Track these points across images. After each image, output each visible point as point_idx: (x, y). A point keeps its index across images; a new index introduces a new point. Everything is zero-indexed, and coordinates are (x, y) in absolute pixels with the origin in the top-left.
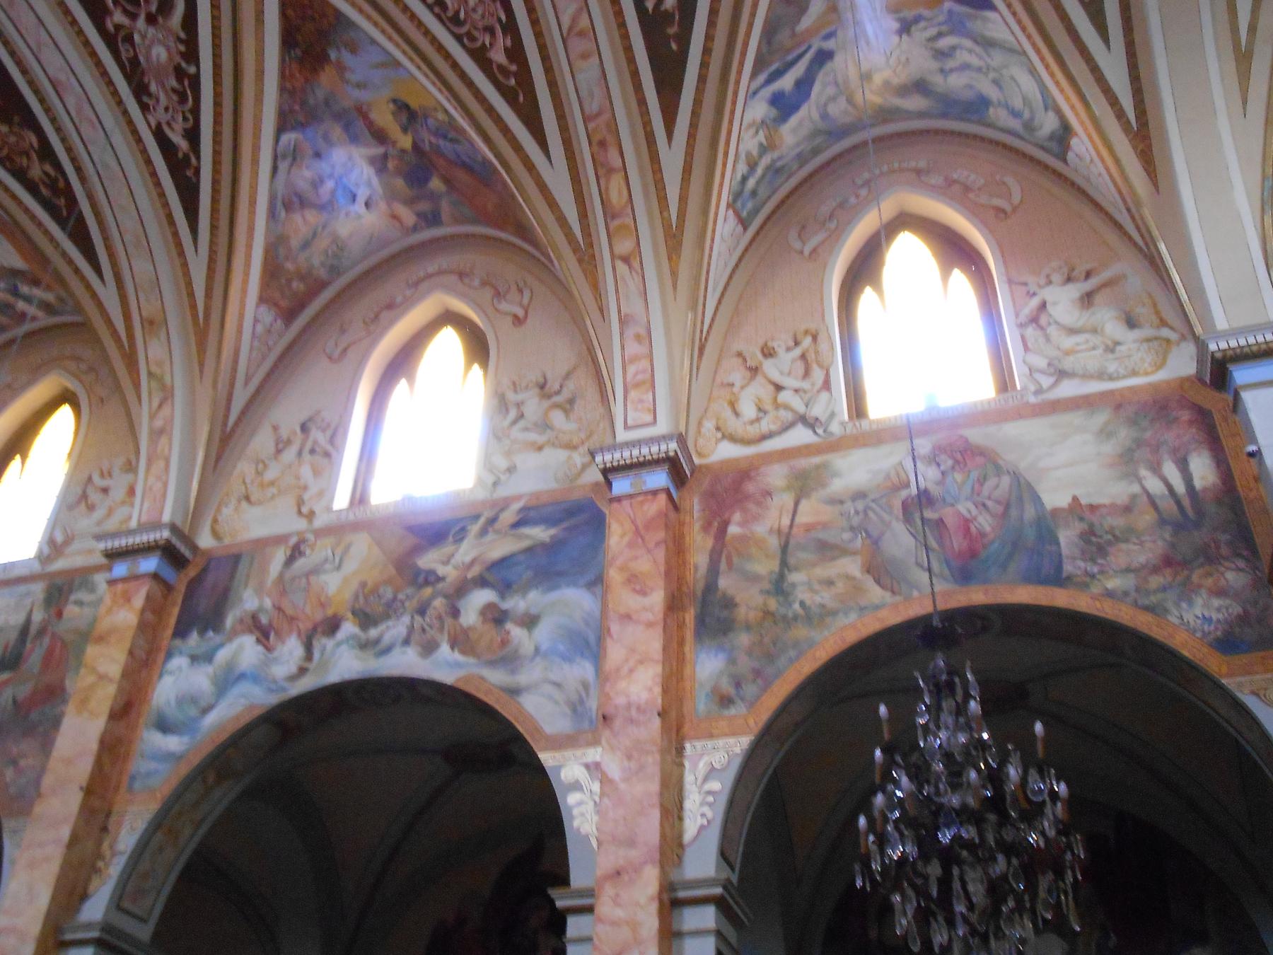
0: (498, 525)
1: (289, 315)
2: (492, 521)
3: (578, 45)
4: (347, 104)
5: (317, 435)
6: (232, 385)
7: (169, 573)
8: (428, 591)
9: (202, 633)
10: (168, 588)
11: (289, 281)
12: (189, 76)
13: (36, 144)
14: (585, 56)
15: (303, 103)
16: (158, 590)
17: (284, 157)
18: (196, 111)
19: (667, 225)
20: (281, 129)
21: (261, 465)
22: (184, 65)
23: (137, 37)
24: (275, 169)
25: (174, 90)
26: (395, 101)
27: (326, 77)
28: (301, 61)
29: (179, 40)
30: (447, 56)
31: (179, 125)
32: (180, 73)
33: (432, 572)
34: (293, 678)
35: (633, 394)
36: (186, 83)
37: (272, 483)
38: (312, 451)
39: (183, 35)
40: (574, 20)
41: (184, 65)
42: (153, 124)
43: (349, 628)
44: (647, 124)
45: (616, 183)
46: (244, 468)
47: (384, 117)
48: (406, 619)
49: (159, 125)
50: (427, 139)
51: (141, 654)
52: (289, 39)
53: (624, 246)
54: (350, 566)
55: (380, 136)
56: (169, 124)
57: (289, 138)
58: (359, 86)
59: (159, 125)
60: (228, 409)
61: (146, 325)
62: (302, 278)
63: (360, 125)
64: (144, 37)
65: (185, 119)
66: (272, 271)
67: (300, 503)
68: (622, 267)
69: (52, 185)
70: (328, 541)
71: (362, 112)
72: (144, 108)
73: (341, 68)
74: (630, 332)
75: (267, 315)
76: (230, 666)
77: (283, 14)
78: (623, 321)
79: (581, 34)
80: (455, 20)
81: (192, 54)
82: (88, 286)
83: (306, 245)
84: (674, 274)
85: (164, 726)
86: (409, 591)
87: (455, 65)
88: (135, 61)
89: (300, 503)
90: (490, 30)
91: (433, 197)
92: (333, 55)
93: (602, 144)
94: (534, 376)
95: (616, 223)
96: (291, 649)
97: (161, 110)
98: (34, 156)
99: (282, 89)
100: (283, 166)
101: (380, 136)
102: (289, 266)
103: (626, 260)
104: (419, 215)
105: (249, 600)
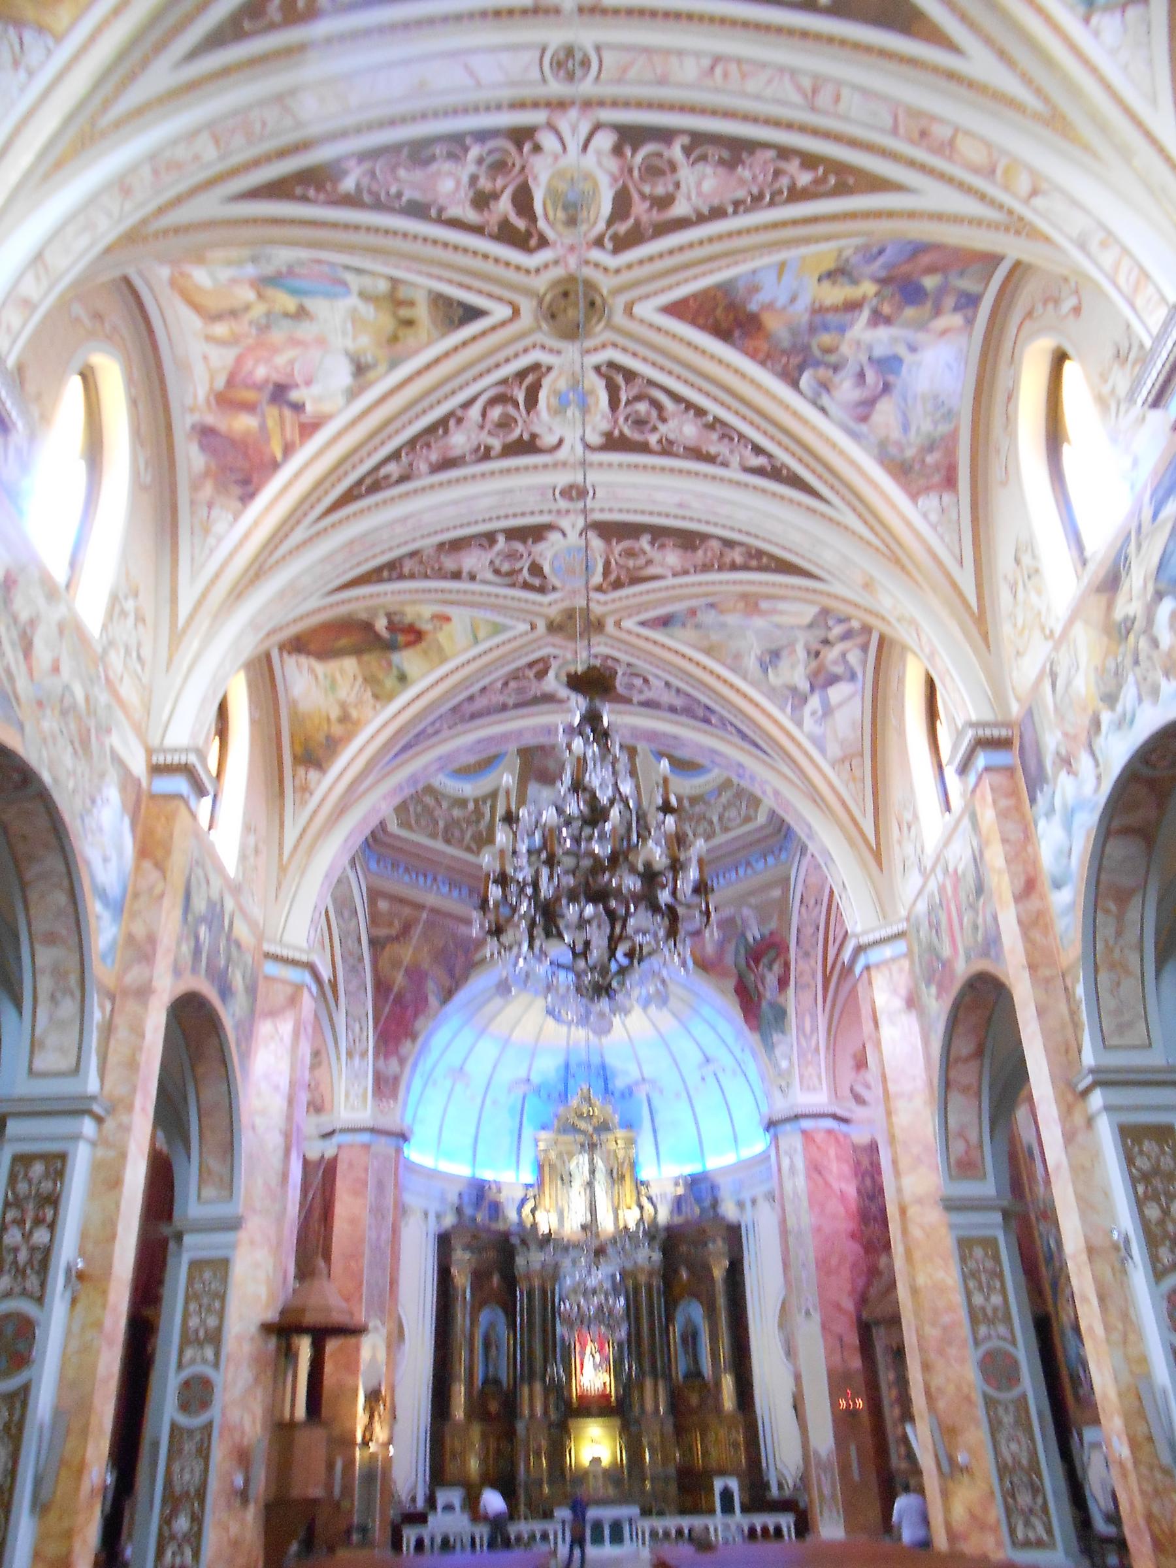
0: (1144, 530)
1: (950, 482)
2: (1140, 527)
3: (824, 99)
4: (805, 318)
5: (1026, 560)
6: (948, 576)
7: (1001, 758)
8: (1132, 638)
9: (1042, 790)
10: (1009, 770)
11: (923, 461)
14: (837, 99)
15: (784, 352)
16: (999, 779)
17: (819, 395)
18: (741, 436)
19: (1036, 117)
20: (795, 384)
21: (1012, 616)
24: (823, 410)
26: (820, 280)
27: (772, 323)
28: (747, 334)
30: (784, 224)
31: (748, 452)
32: (711, 427)
33: (1126, 618)
34: (1097, 789)
35: (1139, 302)
37: (1023, 627)
38: (1029, 577)
40: (799, 88)
43: (1106, 717)
44: (936, 70)
45: (963, 144)
46: (1007, 629)
47: (835, 294)
48: (1131, 678)
50: (877, 268)
51: (1016, 835)
52: (723, 333)
53: (1023, 184)
54: (1083, 660)
55: (853, 306)
57: (806, 380)
58: (793, 299)
60: (961, 595)
62: (931, 447)
63: (831, 318)
66: (901, 470)
67: (1043, 629)
68: (1038, 202)
70: (1064, 648)
71: (818, 310)
72: (725, 464)
73: (770, 307)
74: (1094, 247)
75: (930, 502)
76: (1065, 805)
77: (703, 328)
78: (1082, 246)
79: (815, 91)
80: (757, 199)
81: (700, 412)
83: (906, 427)
84: (1086, 148)
85: (1058, 885)
86: (1121, 649)
87: (795, 222)
89: (1043, 629)
90: (777, 173)
91: (942, 290)
92: (753, 307)
93: (923, 134)
94: (1109, 353)
95: (999, 172)
96: (1084, 763)
99: (763, 363)
100: (825, 400)
101: (853, 306)
102: (910, 453)
103: (1034, 192)
104: (957, 309)
105: (1051, 741)
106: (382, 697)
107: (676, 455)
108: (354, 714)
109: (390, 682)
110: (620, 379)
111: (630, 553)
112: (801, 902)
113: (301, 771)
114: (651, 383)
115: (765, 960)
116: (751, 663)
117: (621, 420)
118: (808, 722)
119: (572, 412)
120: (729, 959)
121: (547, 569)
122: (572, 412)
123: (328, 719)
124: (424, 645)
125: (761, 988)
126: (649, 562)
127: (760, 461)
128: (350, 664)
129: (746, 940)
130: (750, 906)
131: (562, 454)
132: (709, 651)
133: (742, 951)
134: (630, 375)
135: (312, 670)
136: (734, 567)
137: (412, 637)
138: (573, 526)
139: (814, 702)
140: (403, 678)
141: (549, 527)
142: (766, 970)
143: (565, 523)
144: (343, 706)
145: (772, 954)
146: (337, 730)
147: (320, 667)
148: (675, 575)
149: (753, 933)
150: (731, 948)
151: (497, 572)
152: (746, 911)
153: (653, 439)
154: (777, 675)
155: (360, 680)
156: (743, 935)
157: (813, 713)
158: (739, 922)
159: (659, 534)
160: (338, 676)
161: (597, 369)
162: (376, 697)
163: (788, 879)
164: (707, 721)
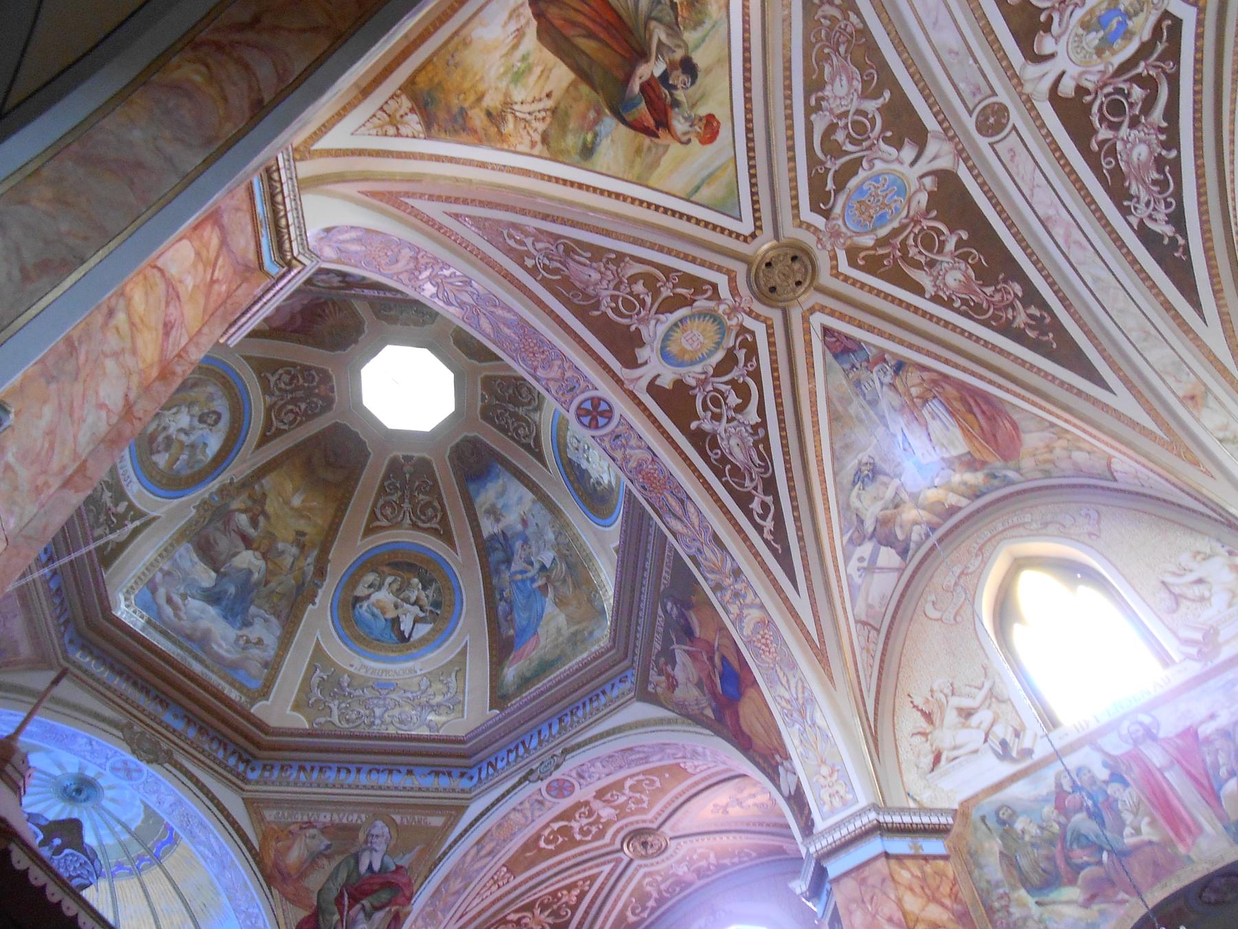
12: (1169, 162)
13: (1020, 294)
18: (1178, 195)
22: (1164, 153)
23: (1119, 146)
25: (1155, 182)
29: (1161, 130)
36: (1167, 168)
39: (1165, 124)
41: (1164, 153)
42: (1135, 222)
49: (1141, 222)
56: (1150, 217)
59: (1141, 222)
61: (1190, 403)
64: (1125, 142)
65: (1168, 205)
69: (1037, 324)
72: (1125, 212)
81: (1172, 141)
82: (1095, 402)
88: (1117, 172)
97: (1142, 206)
98: (1018, 304)
106: (549, 145)
107: (1096, 168)
108: (510, 126)
109: (572, 142)
110: (1160, 47)
111: (929, 241)
112: (478, 843)
113: (406, 103)
114: (1174, 81)
116: (851, 465)
117: (1109, 89)
118: (854, 563)
119: (1094, 39)
120: (315, 881)
121: (853, 183)
122: (1094, 39)
123: (480, 98)
124: (647, 141)
126: (932, 264)
127: (1164, 229)
128: (562, 75)
129: (357, 863)
130: (391, 823)
131: (1031, 71)
132: (834, 418)
133: (343, 876)
134: (1174, 53)
135: (520, 34)
136: (1006, 329)
137: (650, 122)
138: (935, 158)
139: (867, 549)
140: (587, 152)
141: (920, 137)
142: (361, 916)
143: (932, 147)
144: (508, 104)
145: (384, 896)
146: (478, 118)
147: (531, 41)
148: (936, 299)
149: (373, 859)
150: (328, 867)
151: (832, 128)
153: (1104, 133)
154: (859, 496)
155: (549, 104)
156: (357, 858)
157: (861, 559)
158: (361, 836)
159: (982, 235)
160: (537, 71)
161: (1166, 14)
162: (545, 139)
163: (461, 810)
164: (743, 501)
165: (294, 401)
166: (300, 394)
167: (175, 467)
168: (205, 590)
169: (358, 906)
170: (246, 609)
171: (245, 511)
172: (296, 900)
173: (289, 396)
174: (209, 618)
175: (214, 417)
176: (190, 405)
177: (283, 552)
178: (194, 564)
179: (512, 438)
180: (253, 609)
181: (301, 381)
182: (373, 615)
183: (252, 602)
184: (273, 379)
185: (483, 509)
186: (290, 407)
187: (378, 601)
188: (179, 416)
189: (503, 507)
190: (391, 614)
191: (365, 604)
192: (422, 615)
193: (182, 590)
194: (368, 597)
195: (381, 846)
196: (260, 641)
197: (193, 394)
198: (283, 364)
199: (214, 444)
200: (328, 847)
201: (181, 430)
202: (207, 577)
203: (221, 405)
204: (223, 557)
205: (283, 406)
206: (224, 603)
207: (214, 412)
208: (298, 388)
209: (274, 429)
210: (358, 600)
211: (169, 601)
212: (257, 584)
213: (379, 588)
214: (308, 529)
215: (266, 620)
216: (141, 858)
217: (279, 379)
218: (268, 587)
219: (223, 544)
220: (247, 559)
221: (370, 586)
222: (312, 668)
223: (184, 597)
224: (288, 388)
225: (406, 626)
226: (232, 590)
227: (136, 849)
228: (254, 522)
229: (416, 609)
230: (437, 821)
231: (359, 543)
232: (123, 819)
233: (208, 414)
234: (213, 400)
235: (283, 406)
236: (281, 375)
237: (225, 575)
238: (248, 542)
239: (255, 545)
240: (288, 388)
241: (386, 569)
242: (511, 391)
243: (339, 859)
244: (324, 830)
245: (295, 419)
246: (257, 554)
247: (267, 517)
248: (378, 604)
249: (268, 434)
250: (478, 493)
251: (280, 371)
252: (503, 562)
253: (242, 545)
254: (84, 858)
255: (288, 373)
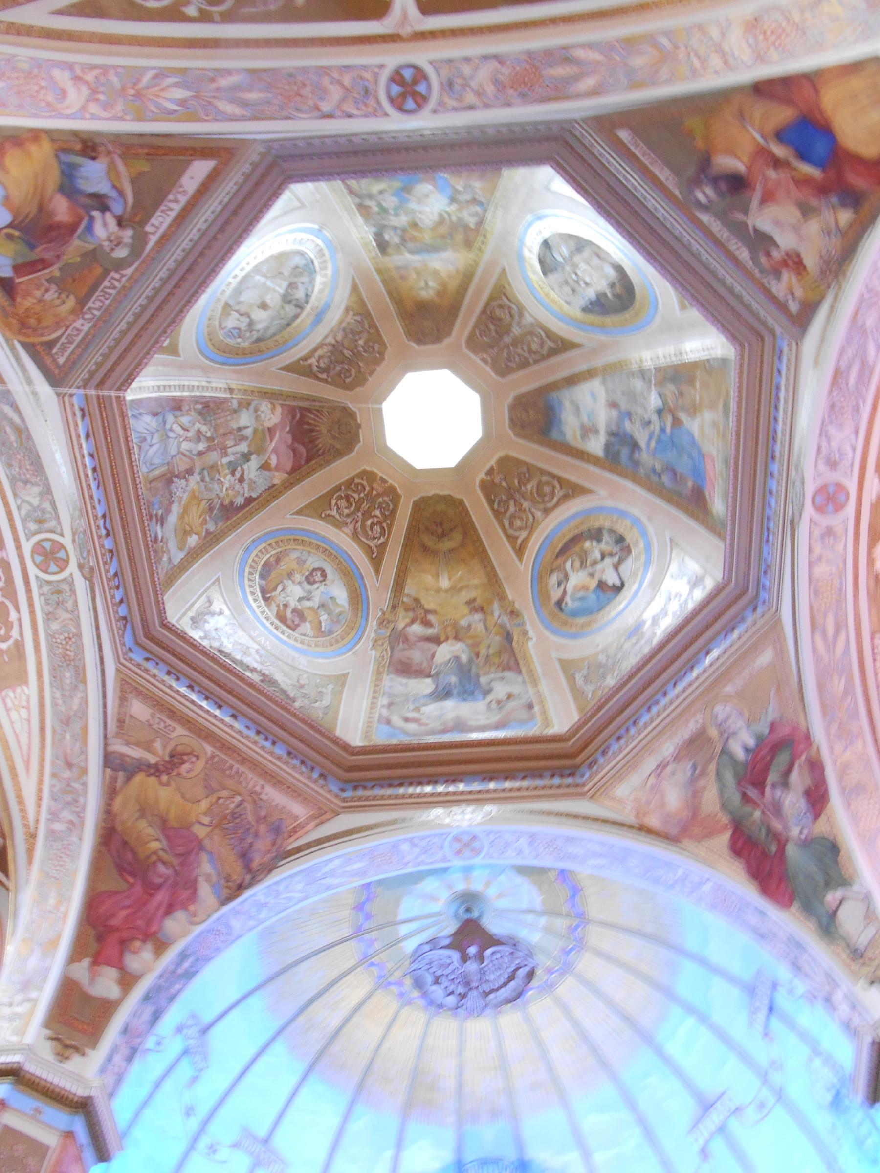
112: (813, 626)
115: (772, 777)
120: (710, 801)
125: (777, 826)
129: (732, 757)
133: (729, 777)
142: (778, 793)
145: (782, 759)
152: (721, 711)
156: (725, 751)
158: (713, 732)
165: (367, 514)
166: (365, 506)
167: (323, 629)
168: (432, 694)
169: (768, 789)
170: (478, 684)
171: (413, 622)
172: (710, 833)
173: (360, 514)
174: (451, 709)
175: (319, 574)
176: (290, 575)
177: (469, 626)
178: (405, 685)
179: (536, 361)
180: (483, 680)
181: (356, 496)
182: (582, 599)
183: (478, 676)
184: (334, 512)
185: (579, 437)
186: (369, 523)
187: (575, 587)
188: (288, 590)
189: (589, 418)
190: (593, 584)
191: (568, 599)
192: (616, 559)
193: (411, 707)
194: (565, 593)
195: (737, 724)
196: (510, 696)
197: (283, 567)
198: (330, 495)
199: (339, 593)
200: (694, 767)
201: (300, 600)
202: (426, 686)
203: (314, 561)
204: (425, 664)
205: (363, 526)
206: (455, 692)
207: (315, 570)
208: (359, 503)
209: (375, 550)
210: (559, 603)
211: (407, 720)
212: (470, 661)
213: (567, 578)
214: (473, 594)
215: (502, 679)
216: (572, 929)
217: (338, 508)
218: (481, 655)
219: (416, 656)
220: (445, 652)
221: (559, 584)
222: (571, 679)
223: (417, 709)
224: (352, 509)
225: (612, 578)
226: (453, 679)
227: (561, 924)
228: (427, 624)
229: (608, 561)
230: (766, 657)
231: (522, 568)
232: (524, 905)
233: (311, 574)
234: (304, 562)
235: (363, 526)
236: (336, 504)
237: (437, 674)
238: (436, 640)
239: (443, 638)
240: (352, 509)
241: (559, 561)
242: (492, 327)
243: (712, 768)
244: (677, 758)
245: (383, 528)
246: (450, 642)
247: (434, 612)
248: (577, 589)
249: (374, 556)
250: (562, 433)
251: (333, 502)
252: (632, 452)
253: (432, 646)
254: (506, 949)
255: (340, 498)
